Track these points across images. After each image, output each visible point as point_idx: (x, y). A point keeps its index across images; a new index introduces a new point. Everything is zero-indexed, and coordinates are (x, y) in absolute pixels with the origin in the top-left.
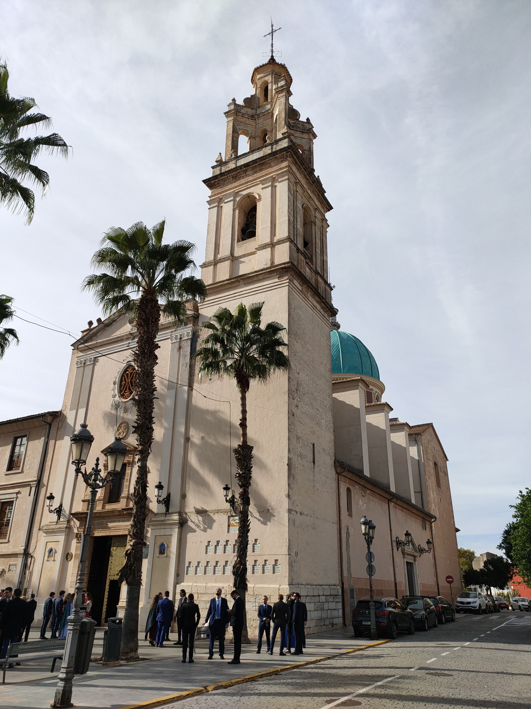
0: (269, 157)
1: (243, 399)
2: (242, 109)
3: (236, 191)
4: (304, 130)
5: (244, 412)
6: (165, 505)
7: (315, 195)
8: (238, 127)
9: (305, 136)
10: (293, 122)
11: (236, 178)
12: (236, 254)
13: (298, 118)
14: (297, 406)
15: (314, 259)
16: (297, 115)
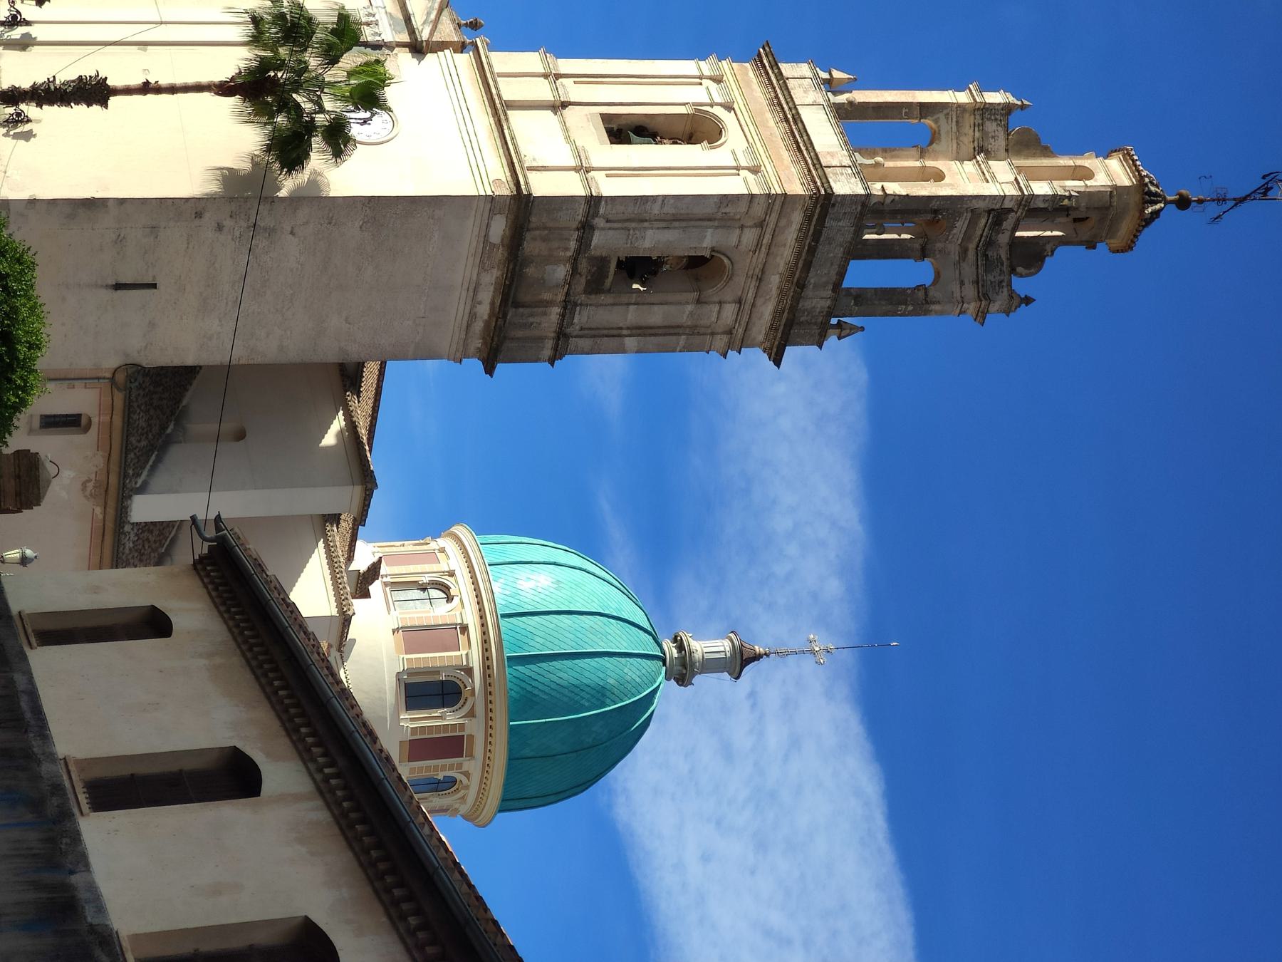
1: (198, 88)
2: (998, 125)
3: (735, 106)
4: (983, 286)
5: (172, 89)
6: (8, 18)
7: (780, 301)
8: (942, 116)
9: (970, 291)
11: (776, 103)
12: (568, 112)
13: (1020, 269)
14: (220, 228)
15: (602, 298)
16: (1026, 267)
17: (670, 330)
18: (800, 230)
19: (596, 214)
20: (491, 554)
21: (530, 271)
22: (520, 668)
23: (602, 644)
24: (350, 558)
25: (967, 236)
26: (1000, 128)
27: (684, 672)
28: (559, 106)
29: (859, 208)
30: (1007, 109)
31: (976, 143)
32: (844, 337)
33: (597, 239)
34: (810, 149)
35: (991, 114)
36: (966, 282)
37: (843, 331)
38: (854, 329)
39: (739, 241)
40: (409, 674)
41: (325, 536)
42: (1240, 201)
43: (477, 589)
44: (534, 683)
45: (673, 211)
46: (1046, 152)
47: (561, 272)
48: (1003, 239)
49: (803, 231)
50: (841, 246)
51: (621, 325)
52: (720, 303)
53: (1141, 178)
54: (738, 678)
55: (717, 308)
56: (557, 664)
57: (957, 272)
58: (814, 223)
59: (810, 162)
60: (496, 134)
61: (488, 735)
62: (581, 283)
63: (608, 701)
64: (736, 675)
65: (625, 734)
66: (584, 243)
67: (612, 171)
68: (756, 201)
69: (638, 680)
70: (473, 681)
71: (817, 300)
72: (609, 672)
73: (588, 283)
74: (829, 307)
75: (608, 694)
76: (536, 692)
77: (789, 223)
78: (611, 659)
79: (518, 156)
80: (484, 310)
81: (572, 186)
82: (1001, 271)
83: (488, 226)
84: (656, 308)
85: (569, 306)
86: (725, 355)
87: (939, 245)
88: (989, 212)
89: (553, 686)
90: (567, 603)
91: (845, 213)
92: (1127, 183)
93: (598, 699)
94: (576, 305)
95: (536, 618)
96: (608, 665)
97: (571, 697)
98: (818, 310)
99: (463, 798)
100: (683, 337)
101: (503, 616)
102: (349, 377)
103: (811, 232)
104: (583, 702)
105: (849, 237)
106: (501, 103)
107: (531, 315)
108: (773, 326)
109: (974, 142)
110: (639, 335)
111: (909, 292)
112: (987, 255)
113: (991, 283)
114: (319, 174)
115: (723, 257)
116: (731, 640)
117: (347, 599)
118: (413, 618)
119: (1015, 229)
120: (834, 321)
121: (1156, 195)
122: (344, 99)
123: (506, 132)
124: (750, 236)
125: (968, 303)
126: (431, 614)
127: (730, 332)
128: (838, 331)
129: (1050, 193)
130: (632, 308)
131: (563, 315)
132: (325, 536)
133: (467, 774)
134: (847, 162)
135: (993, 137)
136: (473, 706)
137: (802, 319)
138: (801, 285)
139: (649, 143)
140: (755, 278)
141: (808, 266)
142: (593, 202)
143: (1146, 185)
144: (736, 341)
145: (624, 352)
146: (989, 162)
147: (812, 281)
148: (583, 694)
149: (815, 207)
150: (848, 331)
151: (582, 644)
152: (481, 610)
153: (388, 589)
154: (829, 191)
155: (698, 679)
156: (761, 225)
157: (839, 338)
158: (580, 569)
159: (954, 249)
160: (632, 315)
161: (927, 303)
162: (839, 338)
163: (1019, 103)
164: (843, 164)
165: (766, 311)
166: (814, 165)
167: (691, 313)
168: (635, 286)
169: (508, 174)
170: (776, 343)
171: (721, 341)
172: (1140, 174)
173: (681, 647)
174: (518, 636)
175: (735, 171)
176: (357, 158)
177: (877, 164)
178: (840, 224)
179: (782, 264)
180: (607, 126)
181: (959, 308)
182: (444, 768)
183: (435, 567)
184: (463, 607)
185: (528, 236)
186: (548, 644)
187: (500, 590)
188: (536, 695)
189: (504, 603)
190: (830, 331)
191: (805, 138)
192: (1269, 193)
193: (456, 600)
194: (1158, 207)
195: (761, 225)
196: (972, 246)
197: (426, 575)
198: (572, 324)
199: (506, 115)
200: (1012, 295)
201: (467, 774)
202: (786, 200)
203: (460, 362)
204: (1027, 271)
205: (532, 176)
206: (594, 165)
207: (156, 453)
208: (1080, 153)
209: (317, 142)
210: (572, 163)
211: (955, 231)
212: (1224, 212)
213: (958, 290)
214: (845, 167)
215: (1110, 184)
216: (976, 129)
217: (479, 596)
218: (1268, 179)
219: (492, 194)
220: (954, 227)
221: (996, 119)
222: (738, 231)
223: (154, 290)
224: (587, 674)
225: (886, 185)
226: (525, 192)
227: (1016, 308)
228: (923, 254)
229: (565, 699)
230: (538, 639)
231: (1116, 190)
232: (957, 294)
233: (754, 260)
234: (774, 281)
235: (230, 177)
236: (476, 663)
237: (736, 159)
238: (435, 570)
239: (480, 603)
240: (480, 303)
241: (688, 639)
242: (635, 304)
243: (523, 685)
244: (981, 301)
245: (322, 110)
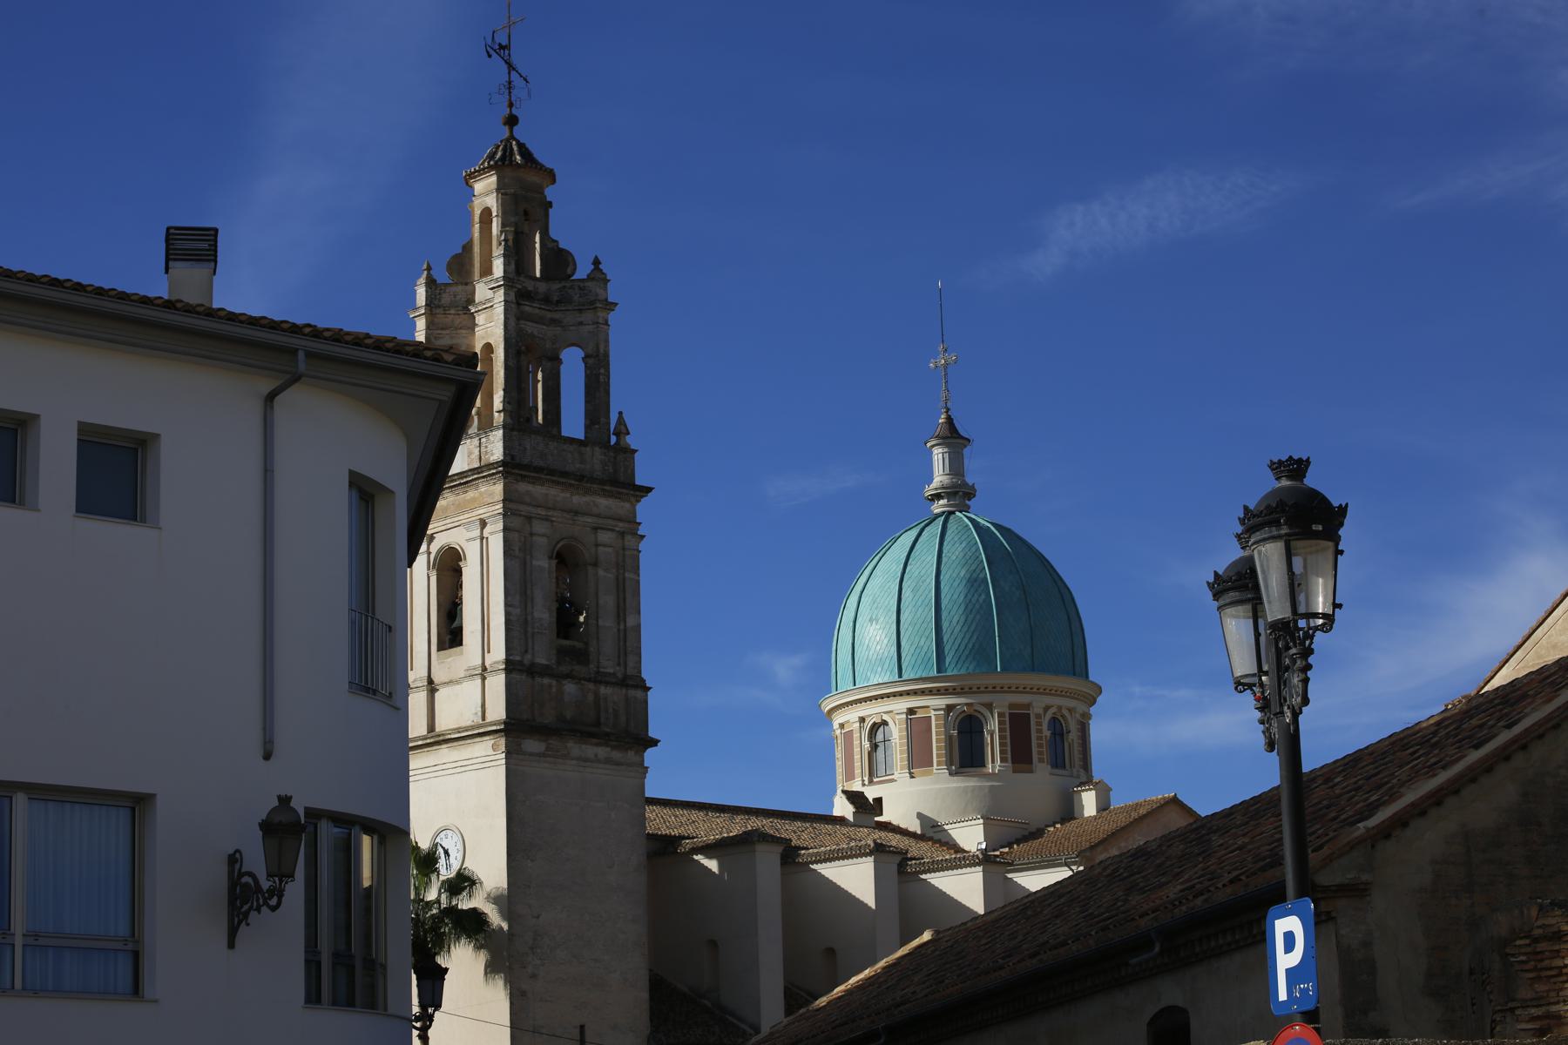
0: (473, 475)
4: (584, 305)
9: (588, 316)
10: (559, 286)
12: (436, 679)
13: (569, 271)
14: (534, 976)
18: (533, 483)
19: (521, 663)
20: (845, 682)
21: (569, 715)
22: (948, 660)
23: (928, 581)
24: (841, 821)
25: (539, 321)
26: (447, 291)
27: (961, 493)
28: (432, 687)
29: (515, 433)
30: (431, 283)
31: (460, 312)
32: (627, 430)
34: (465, 474)
35: (436, 299)
36: (580, 320)
37: (622, 430)
39: (543, 535)
40: (951, 765)
41: (808, 863)
42: (511, 67)
43: (876, 698)
44: (962, 647)
46: (468, 248)
47: (570, 688)
48: (543, 287)
49: (534, 481)
50: (548, 444)
51: (615, 630)
52: (597, 545)
53: (490, 168)
54: (969, 441)
55: (601, 548)
56: (945, 625)
57: (571, 328)
58: (527, 474)
59: (476, 476)
60: (455, 744)
61: (1010, 690)
63: (982, 576)
64: (966, 442)
65: (1014, 557)
66: (545, 671)
67: (485, 648)
69: (963, 545)
70: (959, 705)
71: (595, 460)
72: (955, 575)
74: (600, 448)
75: (975, 575)
76: (970, 646)
78: (943, 573)
79: (473, 728)
80: (602, 752)
81: (497, 683)
82: (569, 288)
83: (531, 754)
85: (600, 679)
86: (642, 537)
88: (518, 304)
89: (965, 629)
90: (890, 613)
91: (520, 445)
92: (494, 178)
93: (980, 586)
94: (598, 672)
95: (903, 644)
96: (947, 576)
97: (976, 612)
98: (603, 457)
99: (1070, 710)
100: (626, 575)
101: (900, 676)
102: (665, 848)
103: (536, 475)
104: (981, 601)
106: (428, 738)
108: (618, 496)
109: (458, 314)
110: (625, 615)
111: (588, 372)
112: (558, 302)
113: (581, 297)
114: (489, 895)
115: (557, 549)
116: (933, 446)
117: (860, 847)
118: (901, 759)
119: (535, 278)
120: (613, 439)
121: (504, 150)
122: (428, 884)
123: (453, 736)
124: (539, 527)
125: (598, 317)
126: (897, 741)
127: (622, 534)
128: (622, 436)
129: (502, 260)
130: (601, 623)
131: (607, 683)
132: (808, 863)
133: (1047, 709)
134: (476, 441)
135: (455, 296)
136: (983, 705)
137: (611, 470)
138: (581, 478)
139: (461, 609)
140: (576, 518)
141: (565, 474)
142: (511, 666)
143: (496, 162)
144: (630, 528)
145: (639, 626)
146: (477, 302)
147: (578, 466)
148: (974, 601)
149: (513, 474)
150: (623, 427)
151: (927, 601)
152: (894, 695)
153: (875, 780)
154: (500, 464)
155: (970, 480)
156: (529, 518)
157: (628, 434)
158: (860, 597)
160: (608, 622)
161: (597, 356)
162: (628, 434)
163: (426, 272)
164: (478, 445)
165: (604, 503)
166: (479, 473)
168: (582, 619)
169: (492, 737)
170: (632, 492)
171: (629, 539)
172: (487, 168)
173: (938, 497)
174: (919, 662)
175: (484, 540)
176: (475, 866)
177: (478, 413)
178: (528, 447)
180: (447, 645)
181: (602, 326)
182: (1039, 731)
183: (856, 735)
184: (891, 712)
186: (927, 634)
187: (877, 676)
188: (973, 646)
189: (888, 673)
190: (622, 443)
191: (456, 477)
192: (504, 44)
193: (885, 717)
194: (515, 148)
195: (529, 518)
196: (549, 315)
197: (863, 743)
198: (614, 674)
199: (439, 736)
200: (590, 278)
201: (1047, 709)
202: (507, 499)
203: (647, 768)
204: (571, 264)
205: (489, 719)
206: (480, 662)
207: (727, 1016)
208: (470, 214)
209: (464, 904)
210: (479, 681)
211: (536, 333)
212: (521, 76)
213: (587, 327)
214: (480, 443)
215: (495, 194)
216: (448, 312)
217: (882, 697)
218: (492, 52)
219: (504, 754)
221: (440, 294)
222: (534, 538)
223: (586, 1027)
224: (955, 596)
225: (495, 409)
226: (502, 727)
227: (603, 274)
228: (556, 360)
229: (978, 617)
230: (922, 643)
231: (501, 188)
232: (590, 328)
233: (560, 520)
234: (578, 500)
235: (491, 969)
236: (942, 702)
237: (474, 539)
238: (859, 734)
239: (888, 696)
240: (596, 755)
241: (929, 490)
243: (963, 658)
244: (596, 308)
245: (438, 901)
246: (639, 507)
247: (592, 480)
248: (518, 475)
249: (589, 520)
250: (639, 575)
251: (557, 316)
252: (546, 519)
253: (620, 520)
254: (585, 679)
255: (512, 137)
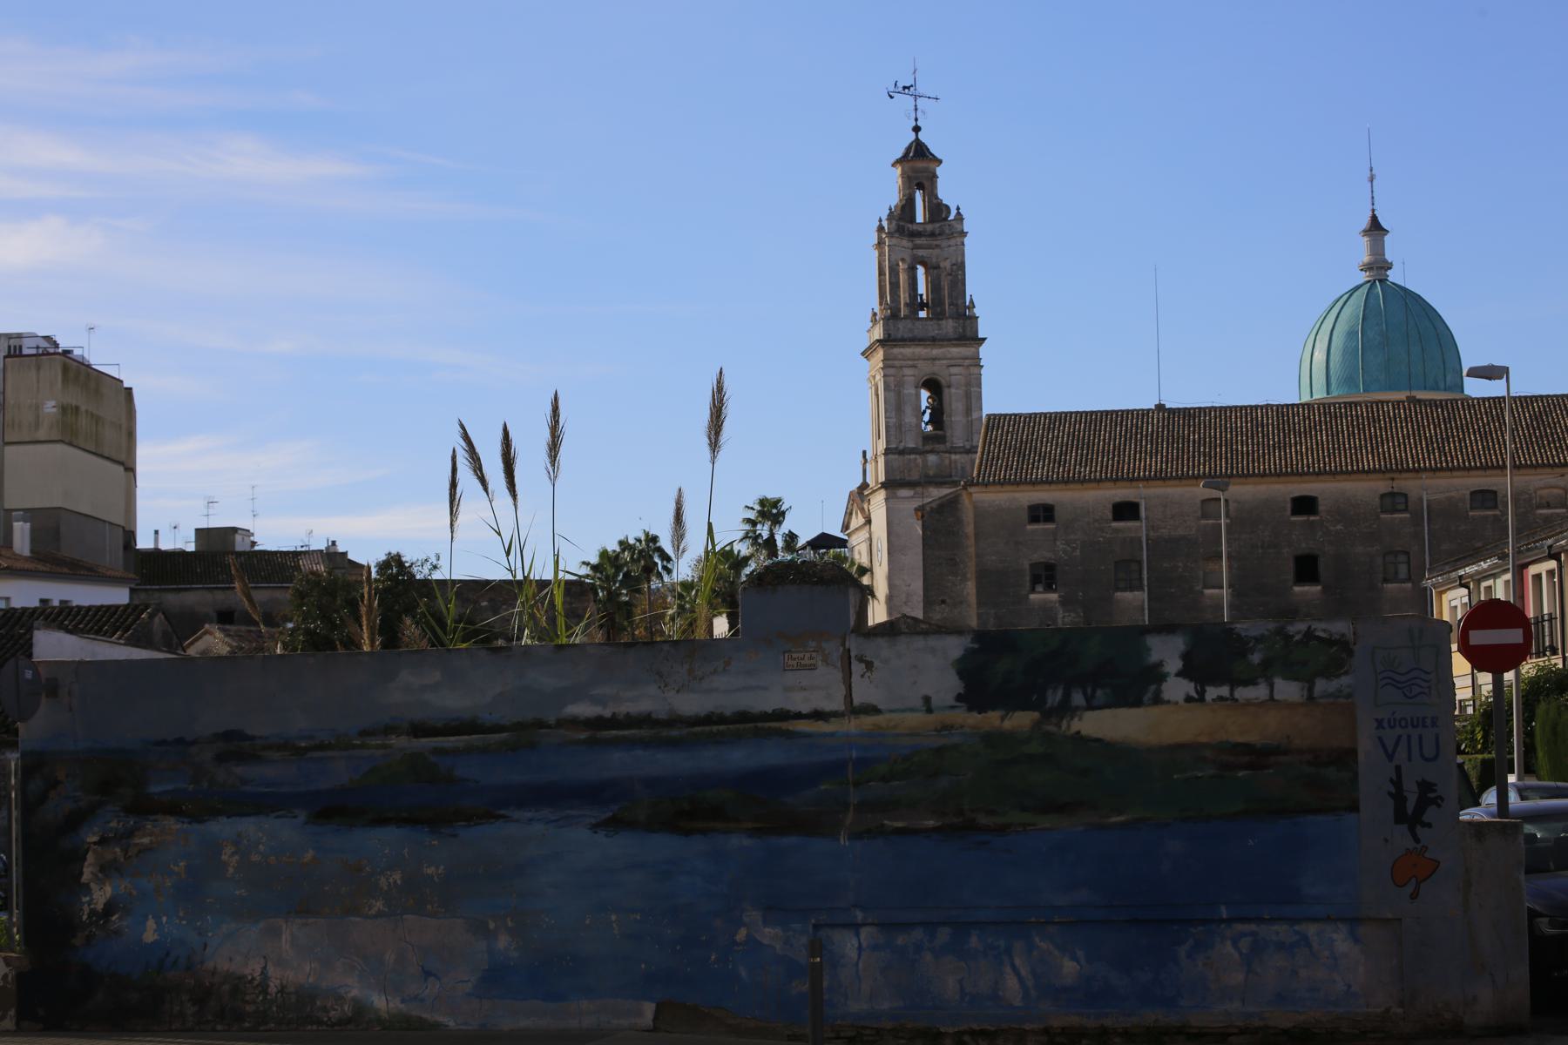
9: (952, 242)
13: (944, 216)
15: (948, 434)
17: (968, 395)
19: (896, 448)
21: (931, 473)
25: (929, 247)
33: (911, 445)
38: (972, 301)
45: (894, 413)
47: (932, 458)
48: (929, 227)
49: (903, 347)
52: (950, 375)
54: (1388, 232)
55: (953, 377)
62: (941, 447)
68: (888, 373)
73: (939, 443)
74: (953, 318)
77: (901, 353)
84: (953, 407)
86: (982, 366)
87: (934, 260)
91: (894, 327)
92: (900, 169)
100: (972, 389)
105: (909, 321)
107: (956, 468)
108: (965, 345)
124: (908, 372)
130: (953, 419)
131: (955, 453)
141: (921, 340)
144: (976, 362)
147: (936, 332)
155: (1389, 257)
159: (937, 251)
162: (974, 307)
165: (955, 351)
167: (957, 388)
171: (974, 370)
179: (925, 351)
185: (907, 478)
195: (901, 367)
196: (935, 243)
198: (964, 447)
211: (925, 255)
220: (922, 256)
222: (905, 378)
234: (936, 352)
242: (951, 416)
246: (981, 349)
247: (950, 340)
248: (895, 345)
249: (945, 362)
250: (981, 388)
251: (938, 242)
252: (914, 366)
253: (966, 358)
254: (943, 452)
255: (917, 139)
